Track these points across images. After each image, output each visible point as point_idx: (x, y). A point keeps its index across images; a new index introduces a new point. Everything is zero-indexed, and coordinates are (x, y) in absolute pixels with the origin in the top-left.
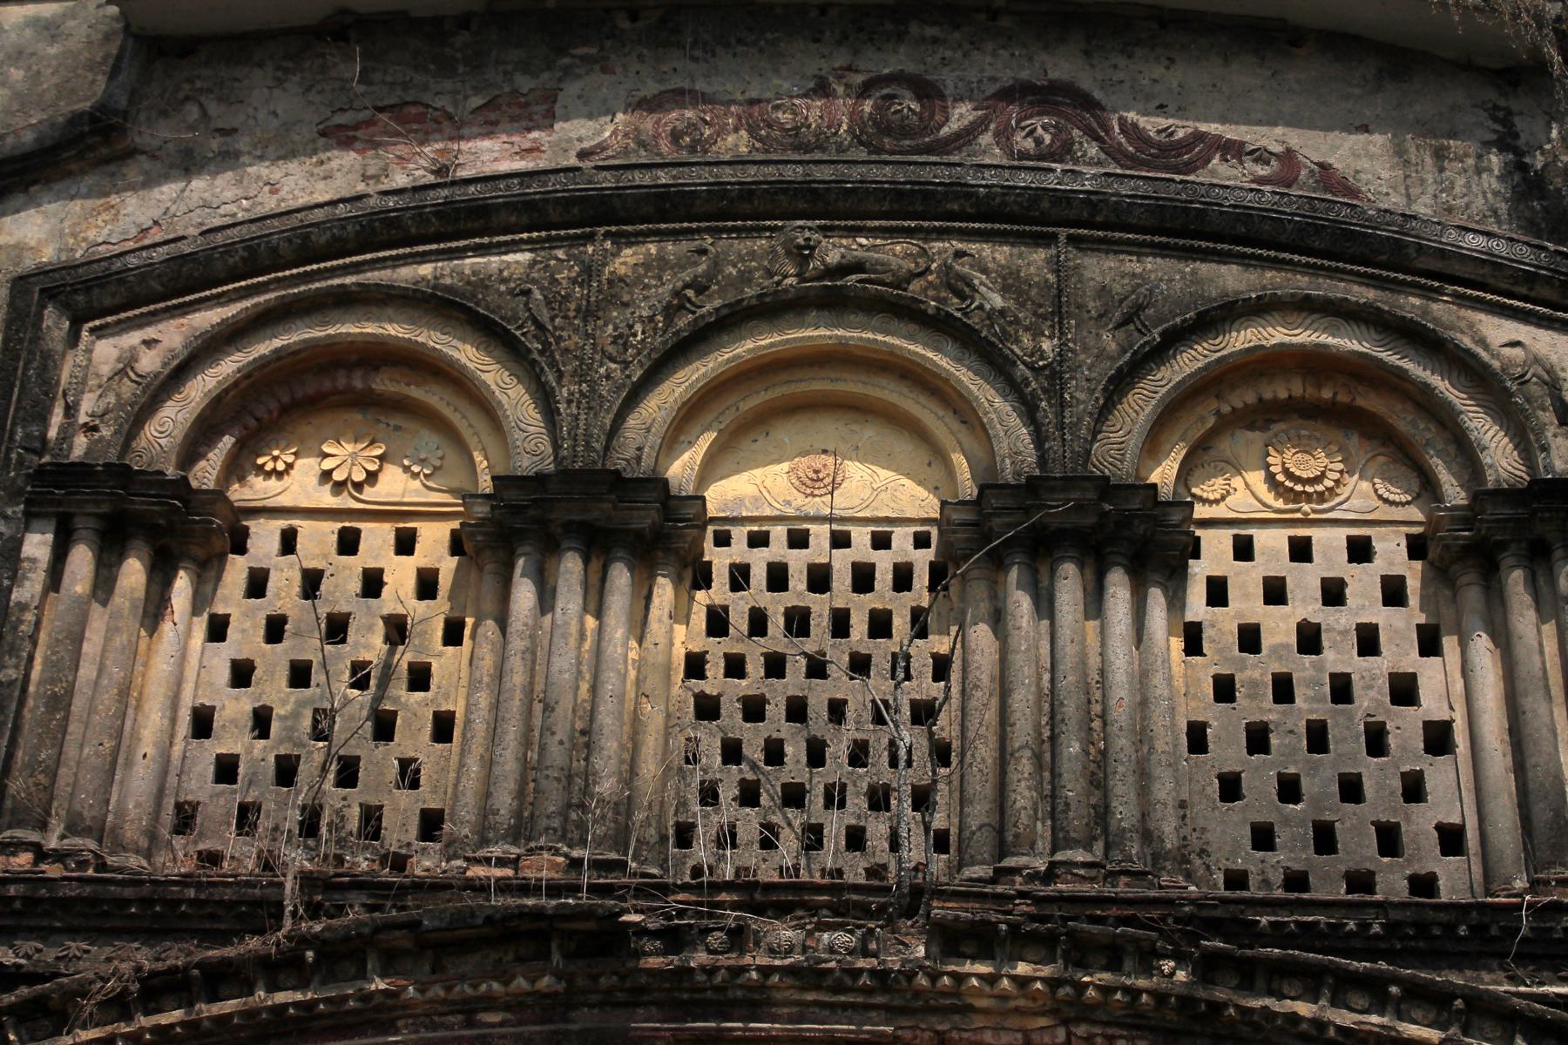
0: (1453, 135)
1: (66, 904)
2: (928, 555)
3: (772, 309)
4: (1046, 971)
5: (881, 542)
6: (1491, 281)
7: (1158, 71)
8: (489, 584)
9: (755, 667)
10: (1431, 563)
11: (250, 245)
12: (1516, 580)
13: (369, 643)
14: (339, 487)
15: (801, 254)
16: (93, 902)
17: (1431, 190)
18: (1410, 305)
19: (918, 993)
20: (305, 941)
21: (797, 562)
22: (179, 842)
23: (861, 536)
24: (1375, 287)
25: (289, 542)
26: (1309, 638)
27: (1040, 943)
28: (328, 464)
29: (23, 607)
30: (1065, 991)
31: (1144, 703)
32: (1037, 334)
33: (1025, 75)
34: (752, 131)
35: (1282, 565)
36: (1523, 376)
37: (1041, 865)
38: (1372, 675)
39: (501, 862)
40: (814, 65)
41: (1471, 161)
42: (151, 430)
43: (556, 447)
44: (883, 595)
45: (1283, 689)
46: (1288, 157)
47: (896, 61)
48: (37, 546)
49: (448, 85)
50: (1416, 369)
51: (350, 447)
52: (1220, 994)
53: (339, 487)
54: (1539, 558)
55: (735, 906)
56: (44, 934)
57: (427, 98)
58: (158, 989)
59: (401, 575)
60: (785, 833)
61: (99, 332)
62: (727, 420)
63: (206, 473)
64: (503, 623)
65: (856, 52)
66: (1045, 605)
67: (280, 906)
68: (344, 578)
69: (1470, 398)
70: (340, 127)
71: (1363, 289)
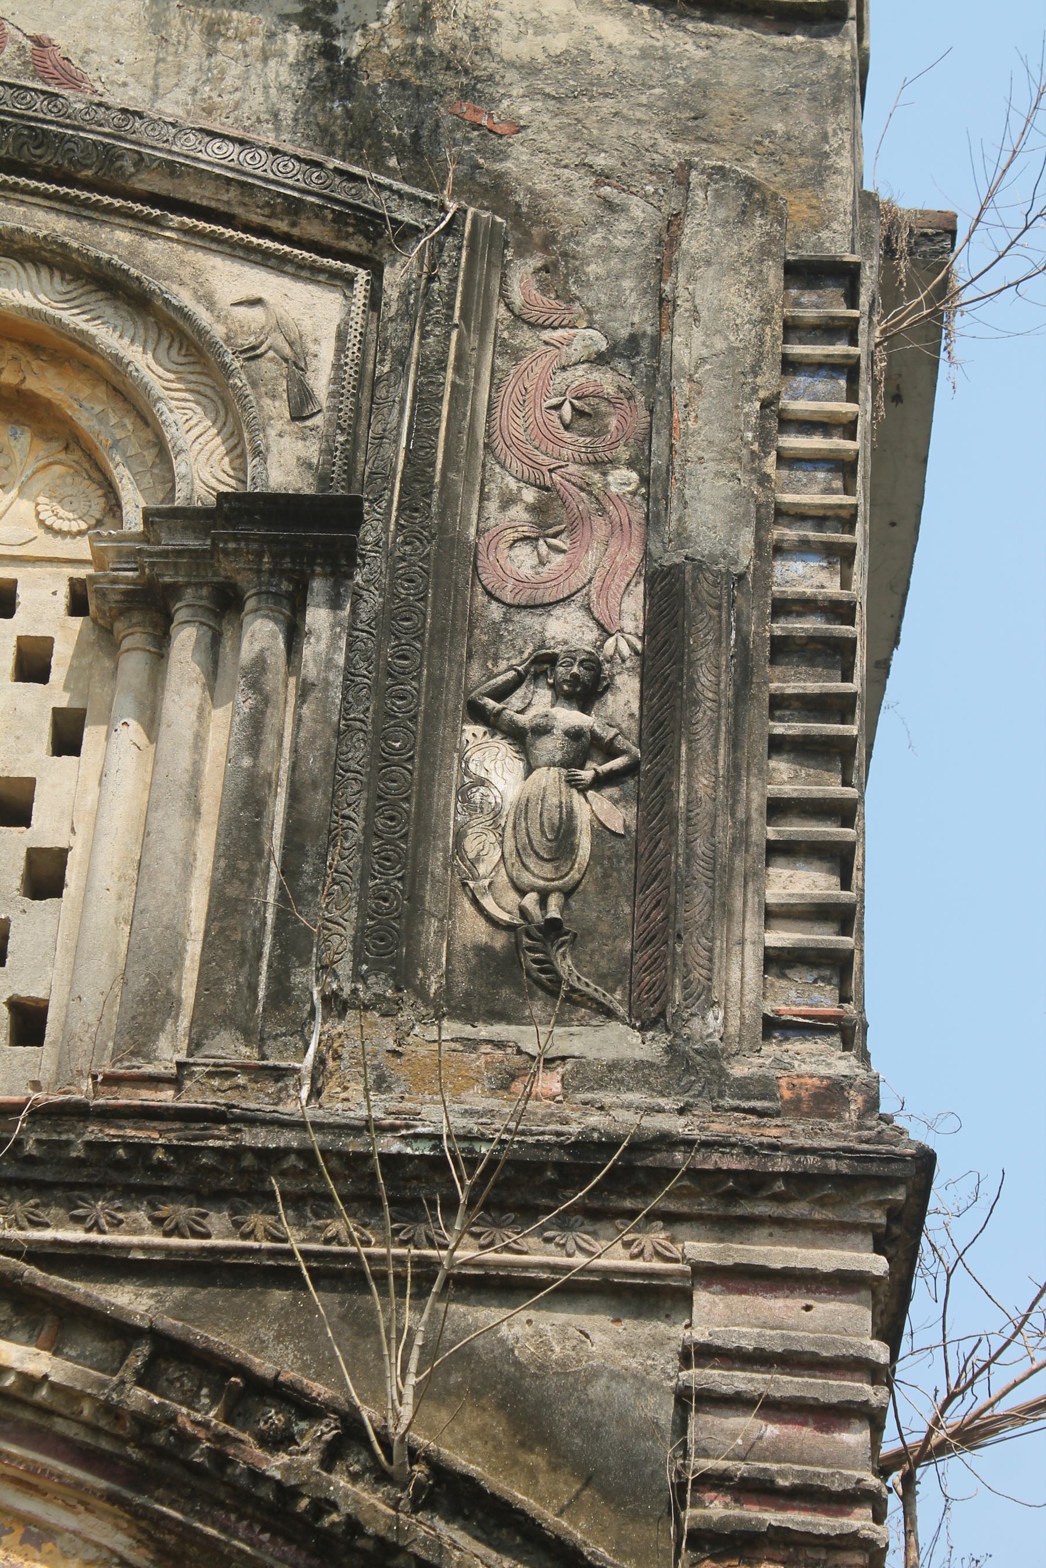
6: (238, 211)
10: (94, 621)
17: (190, 81)
18: (114, 243)
24: (68, 214)
36: (254, 348)
41: (257, 42)
50: (111, 335)
69: (179, 380)
71: (52, 216)
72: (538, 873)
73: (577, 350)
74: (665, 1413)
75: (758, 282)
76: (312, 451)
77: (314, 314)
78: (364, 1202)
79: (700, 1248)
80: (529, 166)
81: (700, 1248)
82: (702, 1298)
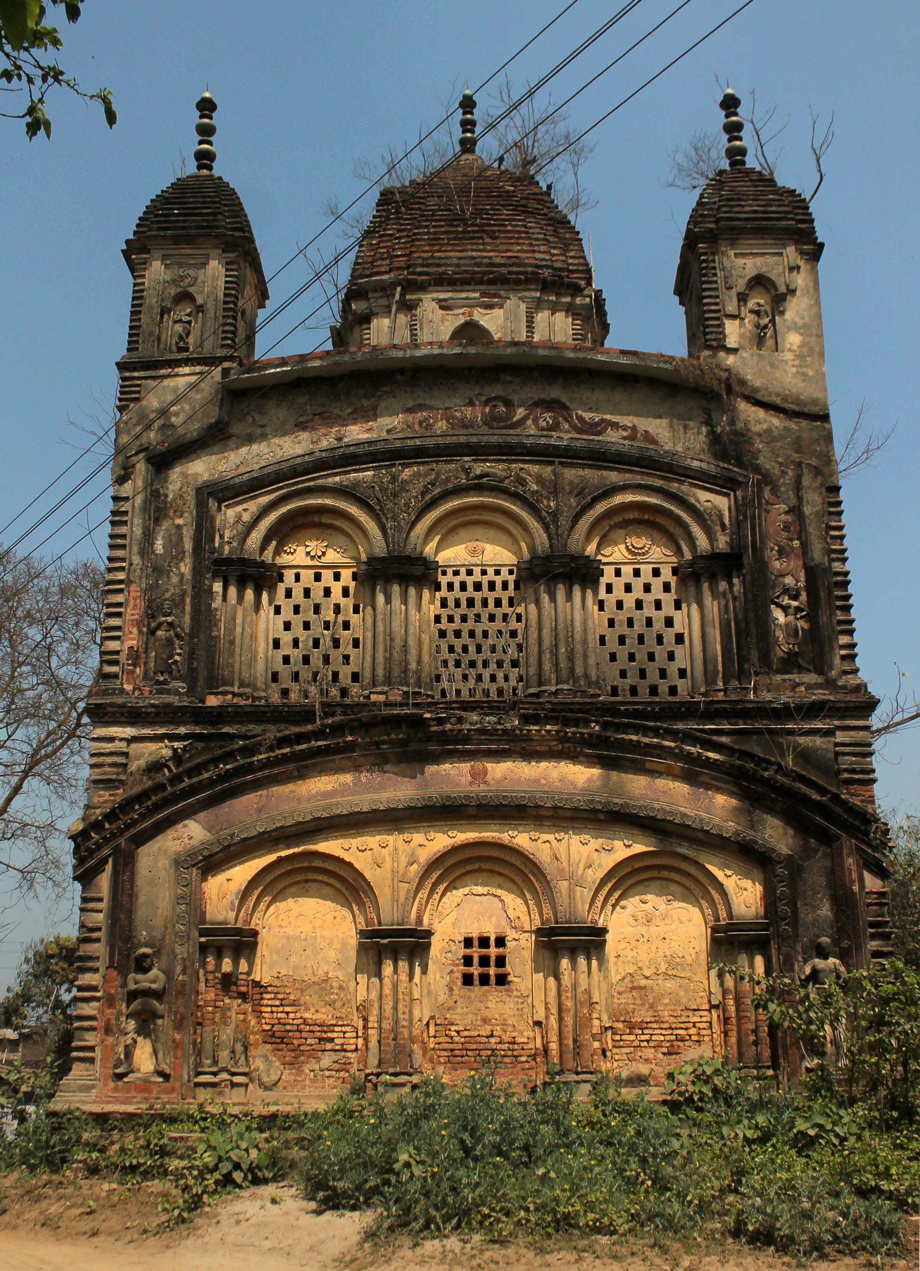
0: (690, 420)
1: (247, 713)
2: (513, 577)
3: (458, 491)
4: (556, 728)
5: (497, 573)
7: (589, 394)
8: (368, 594)
9: (457, 619)
11: (277, 473)
12: (706, 586)
13: (330, 616)
14: (313, 558)
15: (467, 471)
16: (255, 713)
18: (674, 487)
20: (325, 726)
21: (470, 580)
22: (274, 685)
23: (490, 571)
25: (297, 578)
26: (639, 605)
28: (308, 549)
29: (216, 609)
30: (562, 734)
31: (585, 631)
32: (549, 500)
33: (542, 396)
34: (447, 421)
35: (630, 578)
37: (553, 689)
38: (658, 617)
40: (468, 393)
43: (388, 546)
44: (499, 592)
45: (630, 622)
46: (634, 428)
47: (495, 391)
48: (218, 587)
49: (338, 404)
52: (609, 734)
54: (713, 578)
55: (458, 709)
56: (241, 723)
60: (470, 677)
61: (227, 507)
62: (444, 531)
64: (374, 607)
65: (482, 387)
66: (553, 598)
72: (791, 640)
73: (781, 511)
74: (832, 756)
75: (821, 493)
76: (728, 539)
77: (722, 503)
78: (768, 717)
79: (836, 723)
81: (836, 723)
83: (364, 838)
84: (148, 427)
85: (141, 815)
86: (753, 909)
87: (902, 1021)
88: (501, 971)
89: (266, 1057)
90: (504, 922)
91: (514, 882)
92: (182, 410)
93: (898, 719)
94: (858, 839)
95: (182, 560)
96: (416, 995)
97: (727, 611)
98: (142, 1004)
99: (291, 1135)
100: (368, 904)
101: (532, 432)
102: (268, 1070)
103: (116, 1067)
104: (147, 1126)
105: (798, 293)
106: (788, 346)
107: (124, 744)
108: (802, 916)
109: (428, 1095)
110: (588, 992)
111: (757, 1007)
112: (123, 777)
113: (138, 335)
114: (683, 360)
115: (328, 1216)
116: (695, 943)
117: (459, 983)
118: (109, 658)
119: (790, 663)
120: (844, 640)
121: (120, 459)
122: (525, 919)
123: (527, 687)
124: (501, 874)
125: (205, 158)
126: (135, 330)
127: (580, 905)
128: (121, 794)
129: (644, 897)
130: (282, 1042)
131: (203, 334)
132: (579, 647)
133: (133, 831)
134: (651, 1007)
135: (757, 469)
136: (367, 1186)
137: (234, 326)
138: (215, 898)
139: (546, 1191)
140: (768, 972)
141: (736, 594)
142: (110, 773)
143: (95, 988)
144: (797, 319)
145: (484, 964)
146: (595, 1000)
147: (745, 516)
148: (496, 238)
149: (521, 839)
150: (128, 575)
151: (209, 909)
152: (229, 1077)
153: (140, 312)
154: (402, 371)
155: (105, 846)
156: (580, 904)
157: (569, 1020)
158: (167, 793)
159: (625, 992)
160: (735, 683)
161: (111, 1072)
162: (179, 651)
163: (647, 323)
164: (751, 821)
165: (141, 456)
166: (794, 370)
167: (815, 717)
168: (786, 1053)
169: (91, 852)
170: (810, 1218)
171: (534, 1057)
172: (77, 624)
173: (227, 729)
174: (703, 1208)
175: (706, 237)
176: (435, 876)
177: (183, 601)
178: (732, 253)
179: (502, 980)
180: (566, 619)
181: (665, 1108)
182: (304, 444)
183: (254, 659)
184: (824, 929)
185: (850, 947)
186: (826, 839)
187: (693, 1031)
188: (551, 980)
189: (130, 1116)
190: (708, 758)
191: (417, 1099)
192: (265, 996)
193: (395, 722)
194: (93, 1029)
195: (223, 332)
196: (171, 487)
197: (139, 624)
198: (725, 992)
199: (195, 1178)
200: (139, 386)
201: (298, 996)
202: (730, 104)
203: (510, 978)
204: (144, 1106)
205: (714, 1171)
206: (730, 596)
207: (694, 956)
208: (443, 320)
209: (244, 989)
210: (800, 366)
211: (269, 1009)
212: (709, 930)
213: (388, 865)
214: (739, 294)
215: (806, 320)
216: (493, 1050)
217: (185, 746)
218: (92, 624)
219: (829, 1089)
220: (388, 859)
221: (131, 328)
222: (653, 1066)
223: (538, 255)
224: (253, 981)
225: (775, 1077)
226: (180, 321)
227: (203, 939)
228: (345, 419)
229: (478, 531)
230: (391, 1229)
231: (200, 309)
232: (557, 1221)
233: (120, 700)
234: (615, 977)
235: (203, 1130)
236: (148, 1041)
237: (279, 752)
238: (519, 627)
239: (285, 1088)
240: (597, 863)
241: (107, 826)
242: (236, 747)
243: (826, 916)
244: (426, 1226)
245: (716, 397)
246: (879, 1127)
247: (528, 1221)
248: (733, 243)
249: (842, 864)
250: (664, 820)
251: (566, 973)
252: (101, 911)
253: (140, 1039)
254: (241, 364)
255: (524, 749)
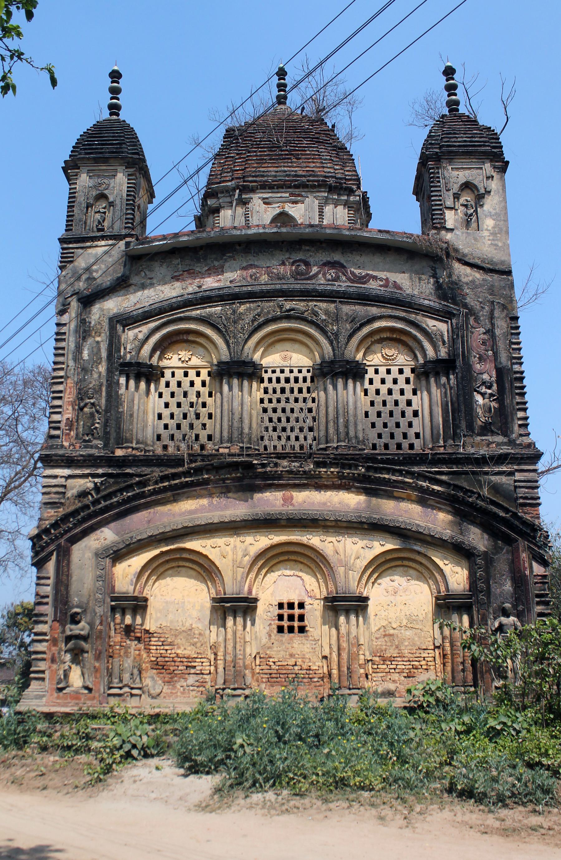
0: (423, 274)
1: (141, 460)
3: (275, 320)
4: (337, 470)
5: (300, 371)
7: (358, 258)
8: (218, 384)
9: (274, 401)
11: (160, 308)
12: (432, 380)
15: (281, 307)
18: (412, 317)
19: (312, 475)
21: (282, 376)
22: (158, 442)
23: (296, 370)
25: (173, 375)
26: (390, 392)
27: (336, 465)
28: (180, 357)
29: (122, 395)
30: (340, 474)
31: (356, 408)
32: (333, 325)
33: (329, 259)
37: (335, 445)
38: (402, 400)
39: (226, 448)
40: (282, 257)
42: (142, 351)
43: (230, 354)
44: (301, 384)
45: (384, 403)
46: (387, 280)
47: (299, 256)
48: (123, 380)
49: (199, 265)
51: (184, 352)
52: (371, 474)
53: (183, 361)
54: (437, 375)
55: (275, 458)
56: (137, 466)
57: (194, 268)
58: (164, 478)
59: (198, 382)
60: (282, 438)
62: (266, 345)
63: (154, 360)
64: (221, 394)
66: (335, 388)
67: (184, 460)
68: (186, 382)
70: (176, 276)
73: (481, 332)
74: (513, 488)
75: (506, 321)
76: (446, 350)
77: (443, 327)
78: (472, 464)
79: (516, 467)
80: (470, 300)
81: (516, 467)
82: (516, 474)
83: (215, 540)
84: (79, 278)
85: (74, 524)
86: (462, 586)
87: (556, 657)
88: (302, 624)
89: (153, 678)
90: (303, 593)
91: (310, 567)
92: (100, 268)
93: (555, 465)
94: (529, 541)
95: (100, 363)
96: (248, 639)
97: (446, 397)
98: (74, 644)
99: (168, 727)
100: (217, 582)
101: (322, 282)
102: (154, 686)
103: (58, 683)
104: (78, 721)
105: (492, 193)
106: (486, 227)
107: (63, 480)
108: (493, 590)
109: (255, 702)
110: (357, 638)
111: (464, 648)
112: (63, 501)
113: (72, 221)
114: (418, 236)
115: (192, 778)
116: (425, 607)
117: (275, 631)
118: (54, 425)
119: (486, 429)
120: (520, 414)
121: (61, 300)
122: (317, 591)
123: (319, 444)
124: (302, 563)
125: (114, 109)
126: (70, 217)
127: (352, 582)
128: (61, 511)
129: (392, 578)
130: (163, 668)
131: (114, 221)
132: (351, 419)
133: (69, 535)
134: (397, 647)
135: (465, 306)
136: (216, 759)
137: (133, 215)
138: (120, 577)
139: (330, 764)
140: (471, 625)
141: (452, 385)
142: (55, 498)
143: (45, 634)
144: (491, 210)
145: (291, 620)
146: (361, 643)
147: (458, 335)
148: (300, 159)
149: (314, 540)
150: (66, 373)
151: (117, 584)
152: (129, 690)
153: (73, 206)
154: (239, 243)
155: (51, 544)
156: (351, 582)
157: (344, 655)
158: (90, 511)
159: (380, 638)
160: (451, 442)
161: (55, 687)
162: (98, 421)
163: (396, 213)
164: (461, 529)
165: (75, 298)
166: (490, 242)
167: (502, 463)
168: (482, 677)
169: (43, 548)
170: (497, 781)
171: (322, 678)
172: (34, 404)
173: (128, 471)
174: (429, 774)
175: (433, 158)
176: (260, 563)
177: (101, 389)
178: (450, 168)
179: (302, 630)
180: (343, 401)
181: (406, 712)
182: (177, 290)
183: (145, 426)
184: (507, 598)
185: (524, 610)
186: (509, 541)
187: (423, 663)
188: (334, 630)
189: (67, 715)
190: (433, 489)
191: (248, 705)
192: (153, 639)
193: (235, 466)
194: (43, 659)
195: (126, 219)
196: (93, 317)
197: (73, 404)
198: (444, 638)
199: (108, 753)
200: (73, 253)
201: (173, 639)
202: (449, 72)
203: (307, 629)
204: (76, 708)
205: (436, 751)
206: (448, 386)
207: (424, 615)
208: (266, 211)
209: (139, 635)
210: (493, 240)
211: (155, 648)
212: (434, 599)
213: (230, 557)
214: (454, 194)
215: (497, 211)
216: (296, 674)
217: (102, 481)
218: (44, 404)
219: (510, 700)
220: (230, 553)
221: (68, 216)
222: (398, 685)
223: (326, 170)
224: (145, 630)
225: (476, 692)
226: (99, 212)
227: (113, 603)
228: (203, 274)
229: (288, 345)
230: (231, 786)
231: (111, 204)
232: (336, 782)
233: (61, 452)
234: (374, 628)
235: (113, 723)
236: (78, 667)
237: (161, 485)
238: (314, 406)
239: (164, 697)
240: (362, 556)
241: (53, 531)
242: (134, 481)
243: (509, 590)
244: (254, 785)
245: (440, 260)
246: (541, 724)
247: (318, 782)
248: (450, 161)
249: (518, 557)
250: (405, 529)
251: (343, 625)
252: (49, 585)
253: (73, 666)
254: (137, 239)
255: (316, 483)
